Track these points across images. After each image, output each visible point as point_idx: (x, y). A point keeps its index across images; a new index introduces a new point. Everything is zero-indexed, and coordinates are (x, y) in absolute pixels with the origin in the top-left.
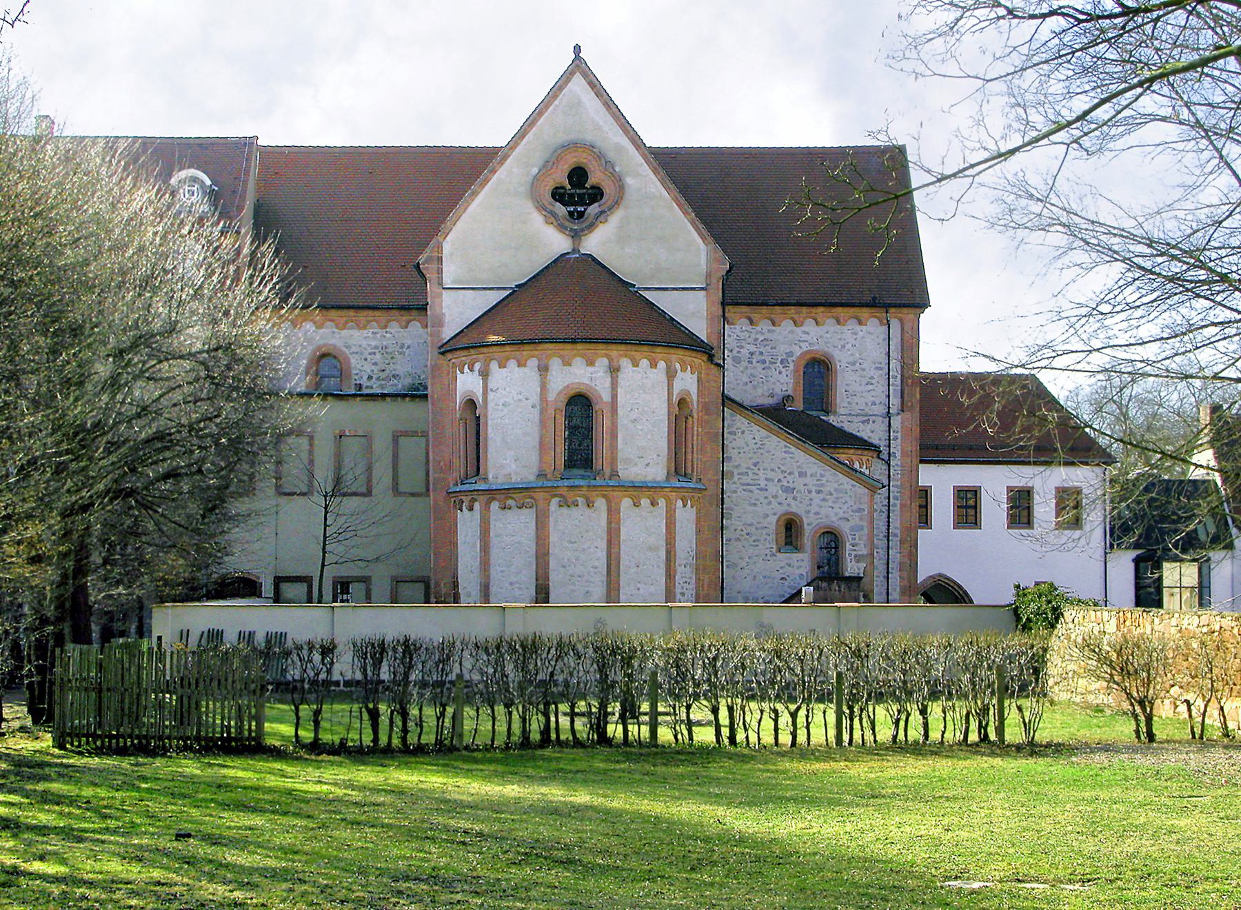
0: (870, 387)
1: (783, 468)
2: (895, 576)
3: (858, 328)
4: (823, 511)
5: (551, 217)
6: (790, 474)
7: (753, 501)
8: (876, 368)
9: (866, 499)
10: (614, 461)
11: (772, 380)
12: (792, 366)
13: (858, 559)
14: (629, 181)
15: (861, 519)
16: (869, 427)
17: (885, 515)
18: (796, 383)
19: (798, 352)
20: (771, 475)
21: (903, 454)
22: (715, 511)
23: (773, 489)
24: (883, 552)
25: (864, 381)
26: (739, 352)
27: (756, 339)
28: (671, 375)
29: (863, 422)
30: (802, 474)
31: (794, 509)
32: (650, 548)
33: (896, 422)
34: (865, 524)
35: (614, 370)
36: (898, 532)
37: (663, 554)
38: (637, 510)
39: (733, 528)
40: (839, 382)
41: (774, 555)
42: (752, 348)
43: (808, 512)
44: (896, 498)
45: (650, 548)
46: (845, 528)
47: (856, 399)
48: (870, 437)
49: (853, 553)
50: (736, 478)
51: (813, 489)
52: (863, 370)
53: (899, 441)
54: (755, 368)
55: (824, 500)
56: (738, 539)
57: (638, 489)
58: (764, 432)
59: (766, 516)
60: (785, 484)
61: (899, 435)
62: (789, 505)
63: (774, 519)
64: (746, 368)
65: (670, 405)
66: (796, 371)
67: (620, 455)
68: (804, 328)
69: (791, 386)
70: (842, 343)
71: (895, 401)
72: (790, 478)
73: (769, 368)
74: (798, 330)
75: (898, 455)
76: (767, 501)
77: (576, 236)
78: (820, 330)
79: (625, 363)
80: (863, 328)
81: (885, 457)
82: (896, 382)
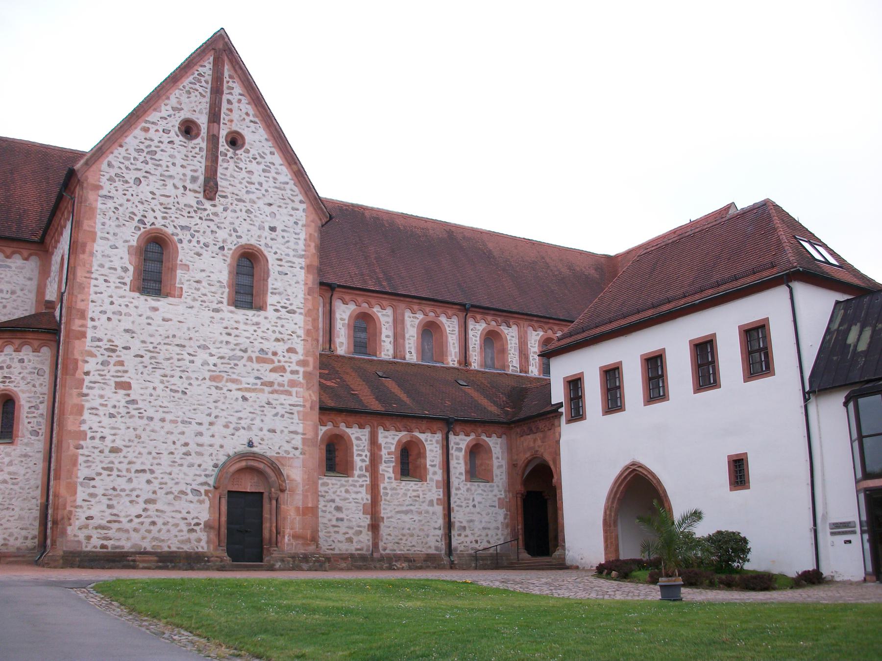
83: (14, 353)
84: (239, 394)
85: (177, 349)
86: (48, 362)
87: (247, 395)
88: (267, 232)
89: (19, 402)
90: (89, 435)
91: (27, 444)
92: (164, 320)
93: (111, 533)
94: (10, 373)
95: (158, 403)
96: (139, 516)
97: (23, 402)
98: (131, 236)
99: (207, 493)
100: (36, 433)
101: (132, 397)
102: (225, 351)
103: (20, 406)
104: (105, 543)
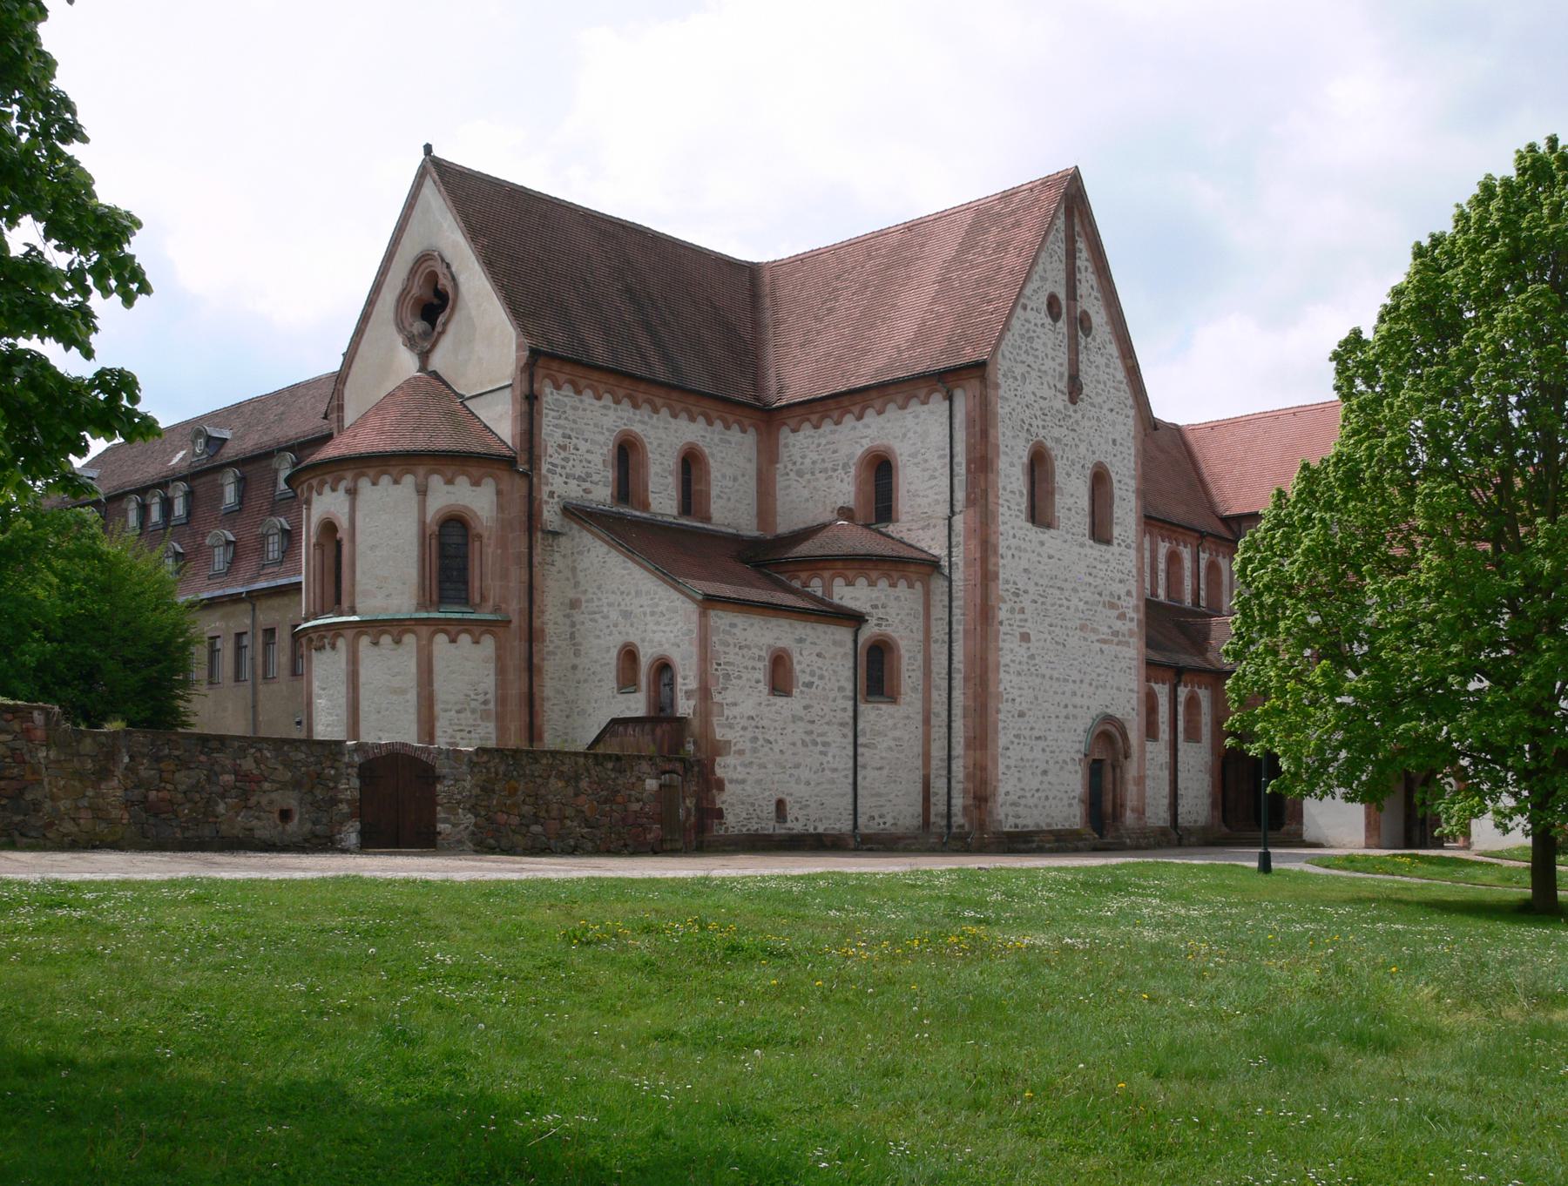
0: (934, 482)
1: (622, 588)
2: (958, 725)
3: (919, 409)
4: (657, 637)
5: (411, 342)
6: (628, 594)
7: (597, 633)
8: (940, 457)
9: (695, 617)
10: (353, 594)
11: (834, 491)
12: (853, 471)
13: (688, 694)
14: (462, 279)
15: (691, 644)
16: (931, 532)
17: (946, 646)
18: (859, 491)
19: (859, 451)
20: (612, 598)
21: (967, 565)
22: (518, 647)
23: (614, 615)
24: (945, 695)
25: (927, 474)
26: (802, 464)
27: (819, 445)
28: (422, 492)
29: (923, 529)
30: (638, 593)
31: (632, 639)
32: (395, 691)
33: (958, 520)
34: (695, 650)
35: (352, 492)
36: (961, 666)
37: (412, 696)
38: (376, 648)
39: (581, 667)
40: (901, 481)
41: (614, 697)
42: (815, 456)
43: (643, 640)
44: (959, 622)
45: (395, 691)
46: (676, 657)
47: (919, 500)
48: (930, 547)
49: (684, 688)
50: (584, 605)
51: (648, 610)
52: (926, 461)
53: (961, 547)
54: (817, 480)
55: (658, 623)
56: (586, 681)
57: (376, 628)
58: (605, 548)
59: (608, 650)
60: (623, 607)
61: (961, 539)
62: (627, 634)
63: (614, 653)
64: (809, 481)
65: (422, 524)
66: (857, 477)
67: (358, 588)
68: (866, 420)
69: (852, 495)
70: (903, 430)
71: (960, 495)
72: (627, 599)
73: (831, 477)
74: (859, 424)
75: (961, 564)
76: (607, 631)
77: (424, 357)
78: (881, 419)
79: (364, 484)
80: (926, 407)
81: (946, 571)
82: (961, 470)
83: (890, 590)
84: (1097, 646)
85: (1058, 592)
86: (921, 601)
87: (1105, 647)
88: (1110, 447)
89: (899, 651)
90: (1005, 696)
91: (909, 704)
92: (1050, 557)
93: (1021, 810)
94: (887, 613)
95: (1047, 658)
96: (1038, 790)
97: (903, 652)
98: (1022, 454)
99: (1080, 760)
100: (914, 689)
101: (1033, 651)
102: (1088, 595)
103: (899, 658)
104: (1018, 821)
